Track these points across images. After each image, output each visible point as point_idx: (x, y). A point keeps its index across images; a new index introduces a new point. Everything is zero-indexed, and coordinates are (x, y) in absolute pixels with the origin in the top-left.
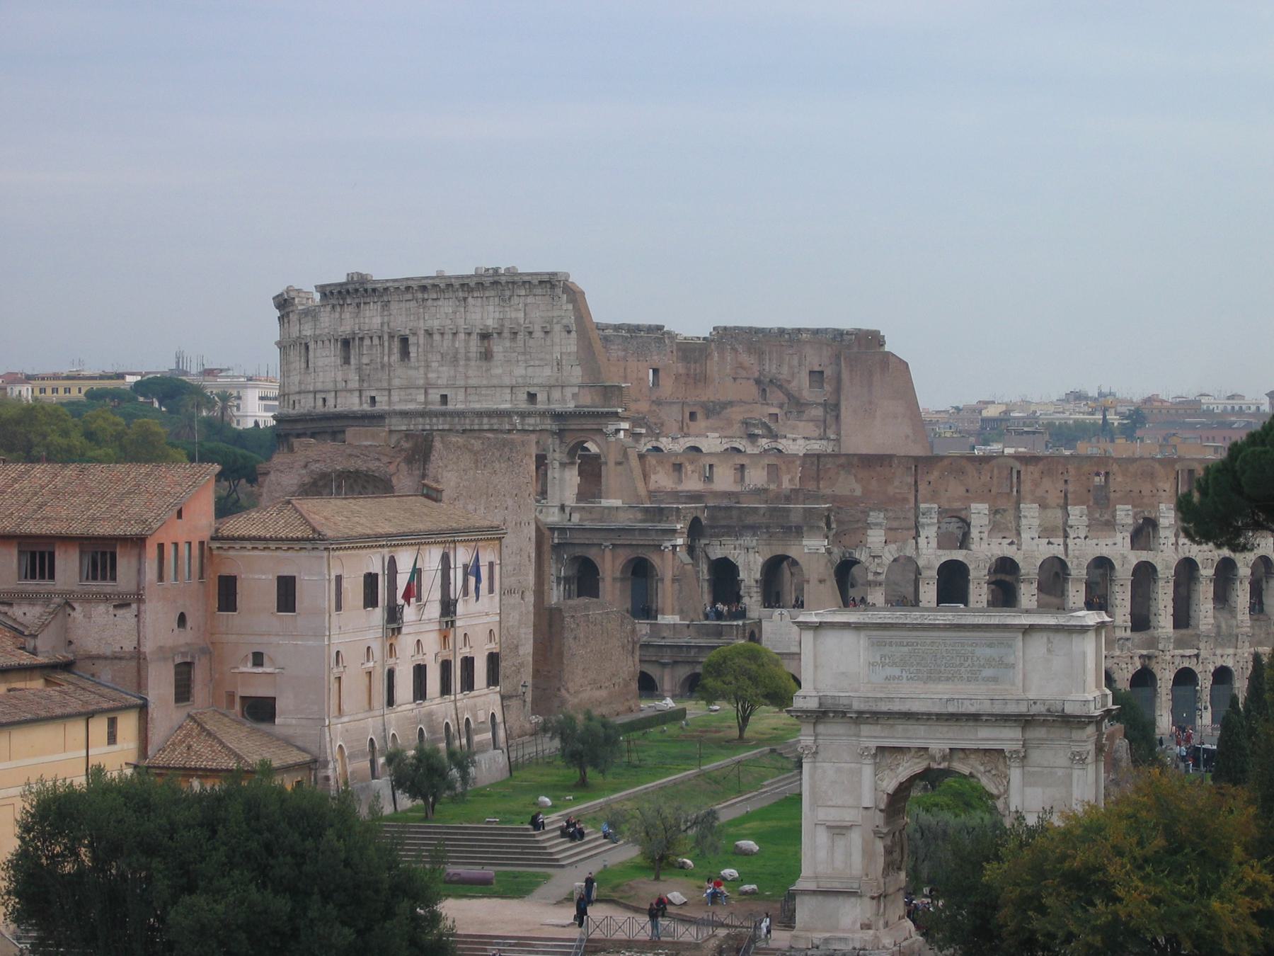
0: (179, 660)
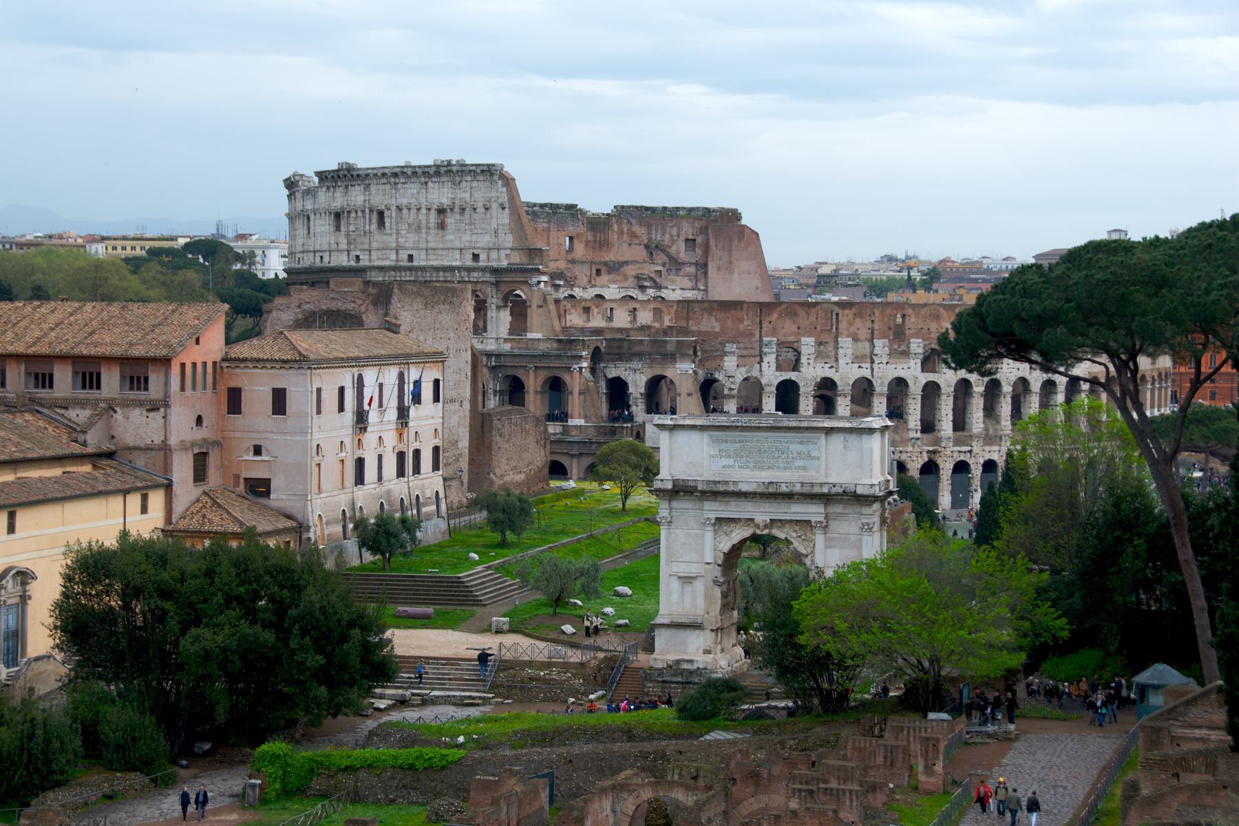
0: (196, 451)
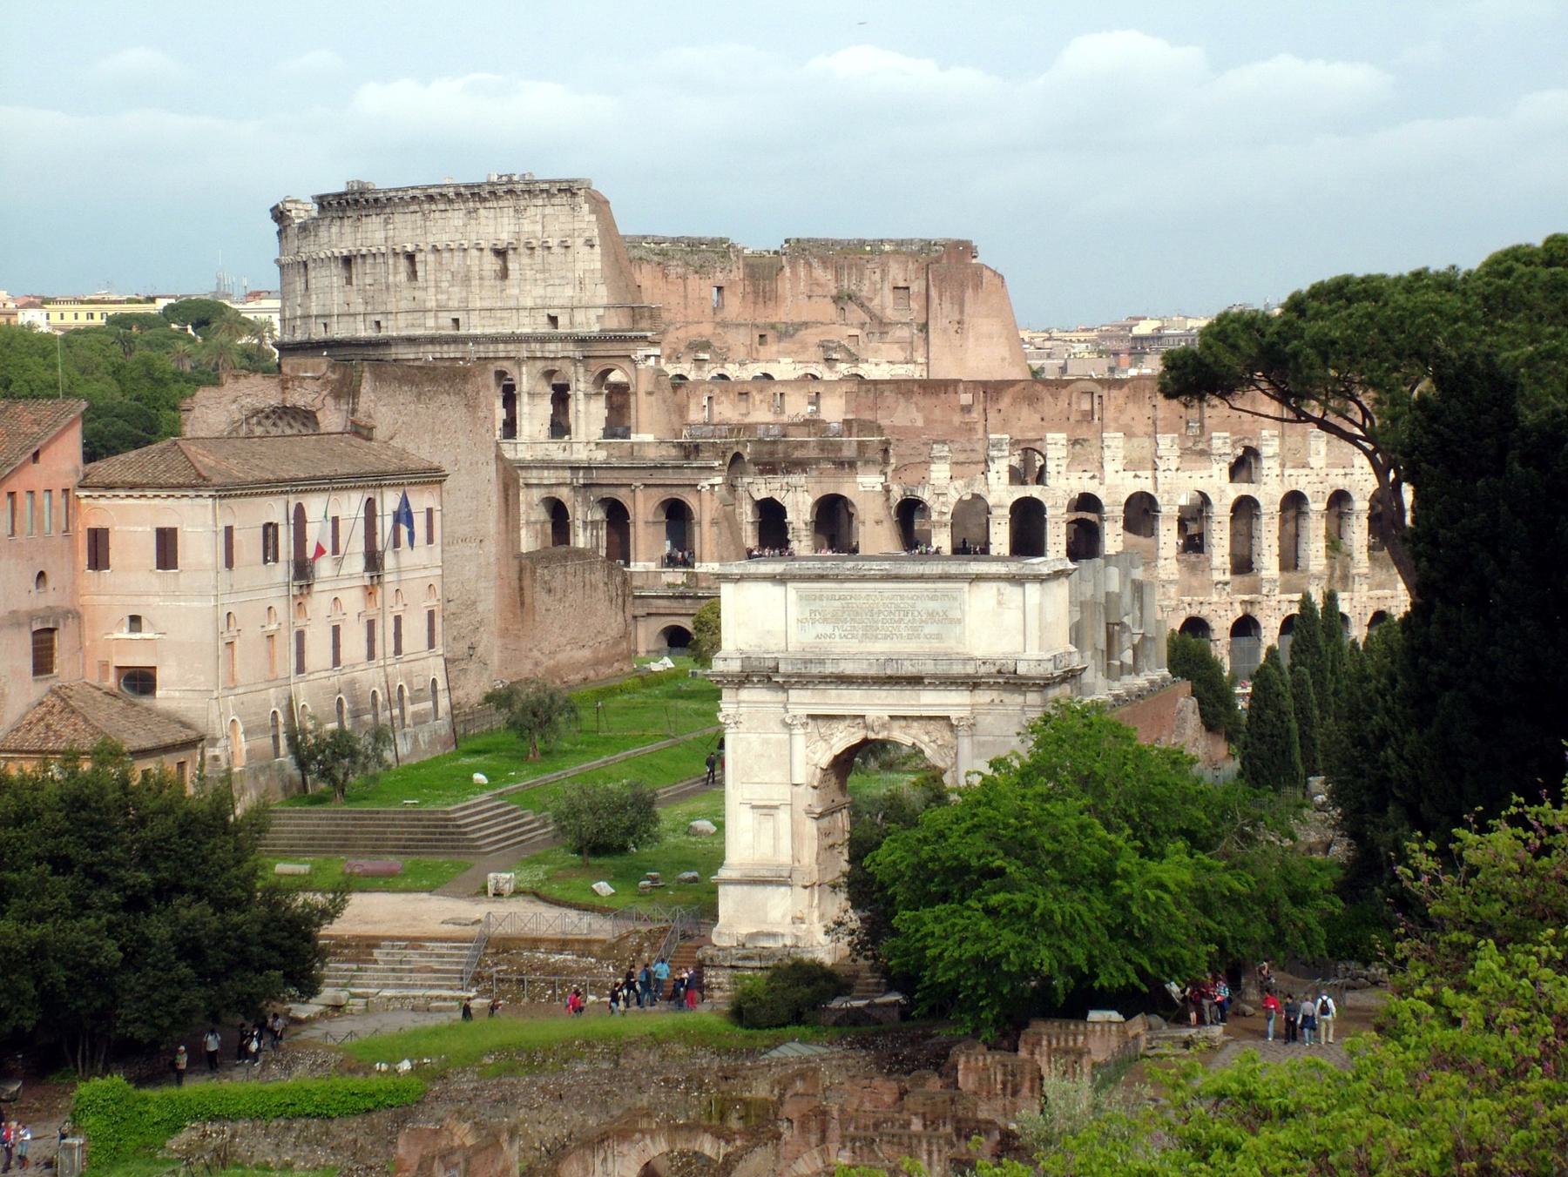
0: (37, 626)
